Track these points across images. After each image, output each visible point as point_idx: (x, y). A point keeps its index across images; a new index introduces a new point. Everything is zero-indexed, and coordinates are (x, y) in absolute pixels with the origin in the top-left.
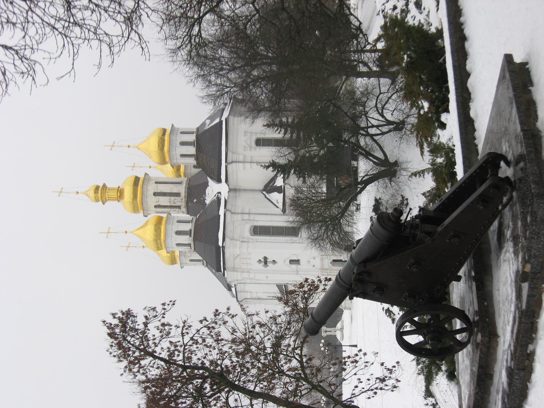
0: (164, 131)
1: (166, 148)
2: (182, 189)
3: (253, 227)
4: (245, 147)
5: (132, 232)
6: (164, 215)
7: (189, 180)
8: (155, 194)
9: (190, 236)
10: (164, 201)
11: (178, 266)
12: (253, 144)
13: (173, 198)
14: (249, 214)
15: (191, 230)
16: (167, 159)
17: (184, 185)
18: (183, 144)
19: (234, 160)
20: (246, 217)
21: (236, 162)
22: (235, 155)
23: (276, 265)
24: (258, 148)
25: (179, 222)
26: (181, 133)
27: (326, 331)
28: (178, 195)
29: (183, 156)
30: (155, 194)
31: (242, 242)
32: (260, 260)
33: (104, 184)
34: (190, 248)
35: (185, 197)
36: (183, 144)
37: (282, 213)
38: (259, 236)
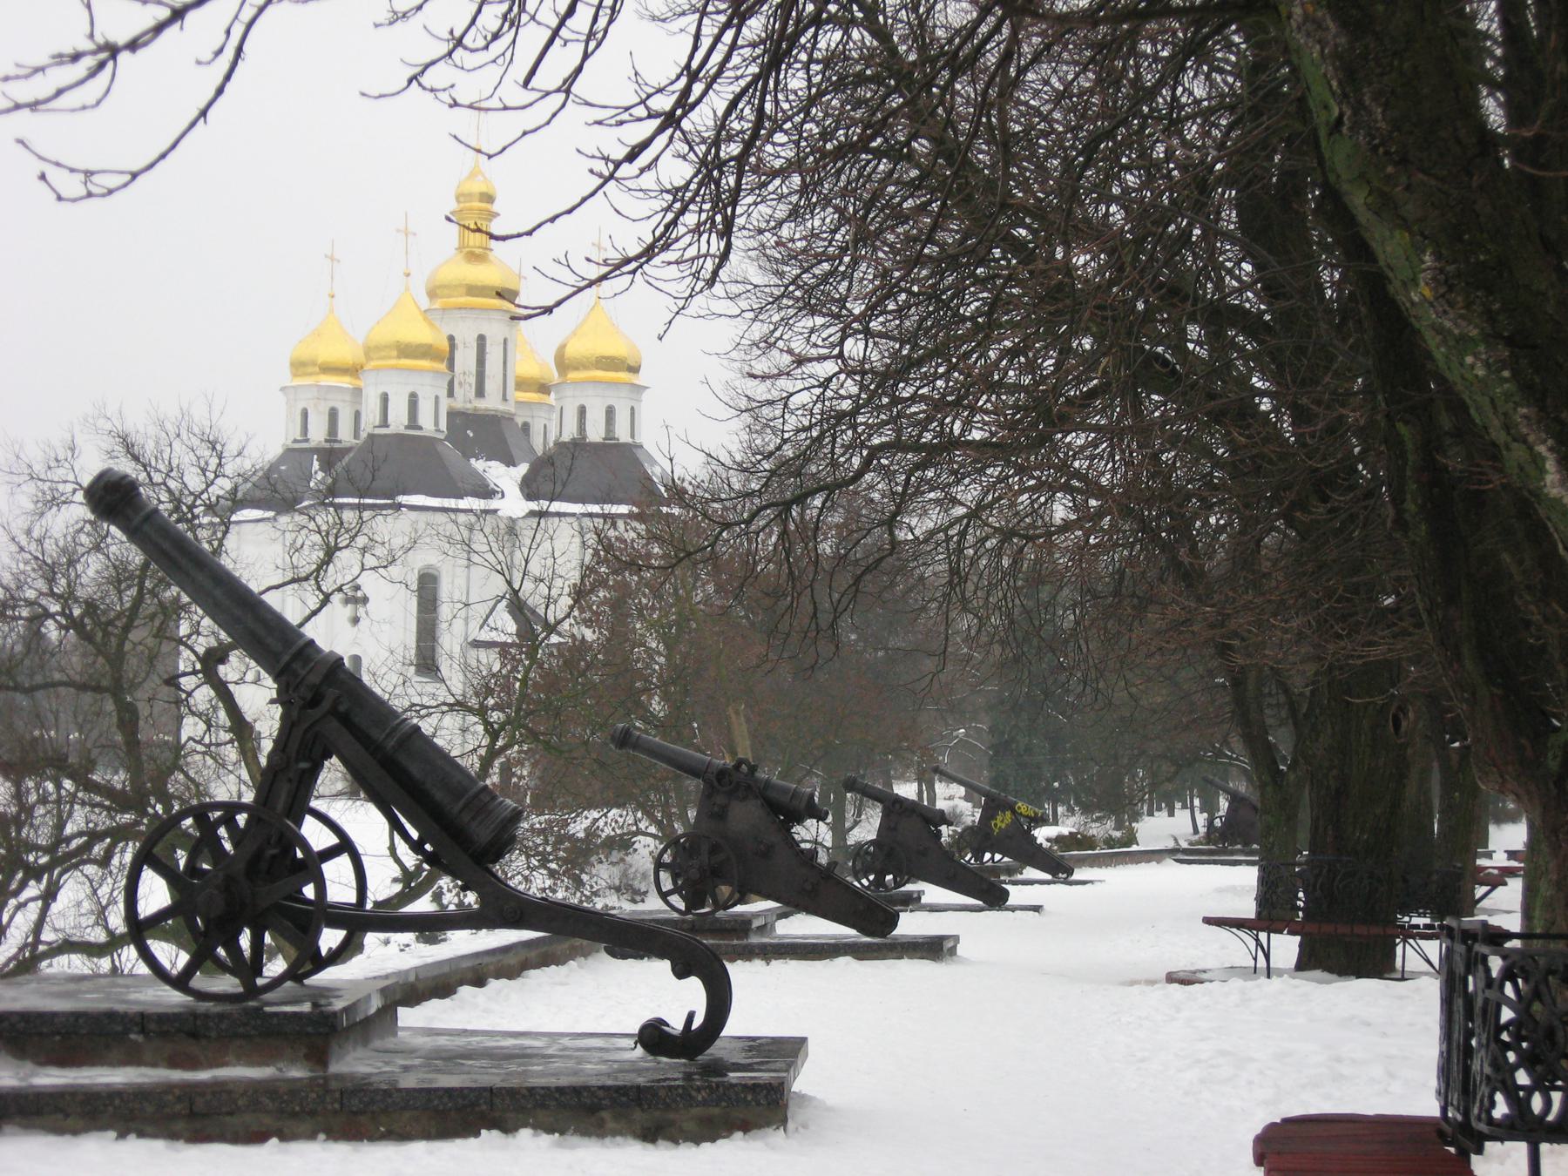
0: (634, 370)
1: (600, 374)
2: (491, 403)
3: (435, 573)
5: (407, 289)
7: (510, 418)
8: (481, 339)
9: (407, 427)
10: (466, 360)
11: (287, 379)
13: (473, 380)
15: (420, 428)
16: (572, 375)
17: (501, 407)
18: (610, 412)
23: (348, 625)
26: (632, 409)
30: (481, 339)
34: (377, 423)
35: (475, 409)
36: (610, 412)
37: (470, 640)
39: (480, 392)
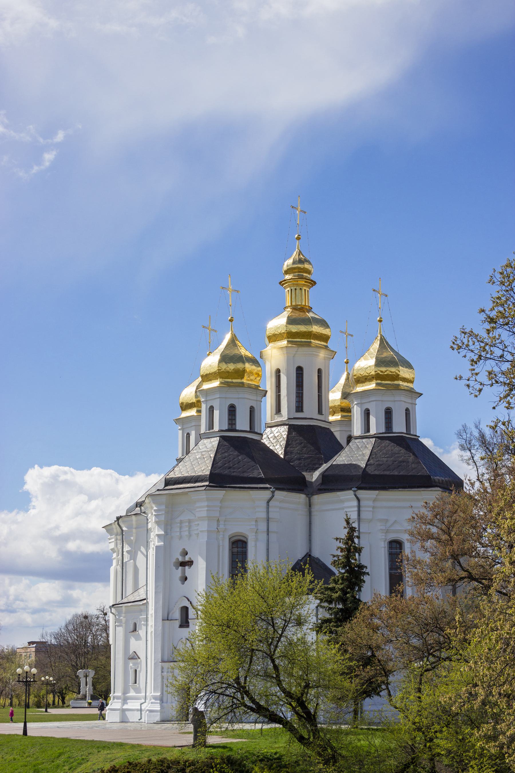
4: (387, 521)
12: (392, 536)
19: (362, 503)
20: (263, 526)
21: (359, 507)
22: (371, 503)
23: (179, 582)
25: (252, 410)
26: (407, 410)
27: (86, 676)
31: (218, 521)
33: (315, 283)
36: (388, 413)
38: (230, 550)
39: (300, 408)
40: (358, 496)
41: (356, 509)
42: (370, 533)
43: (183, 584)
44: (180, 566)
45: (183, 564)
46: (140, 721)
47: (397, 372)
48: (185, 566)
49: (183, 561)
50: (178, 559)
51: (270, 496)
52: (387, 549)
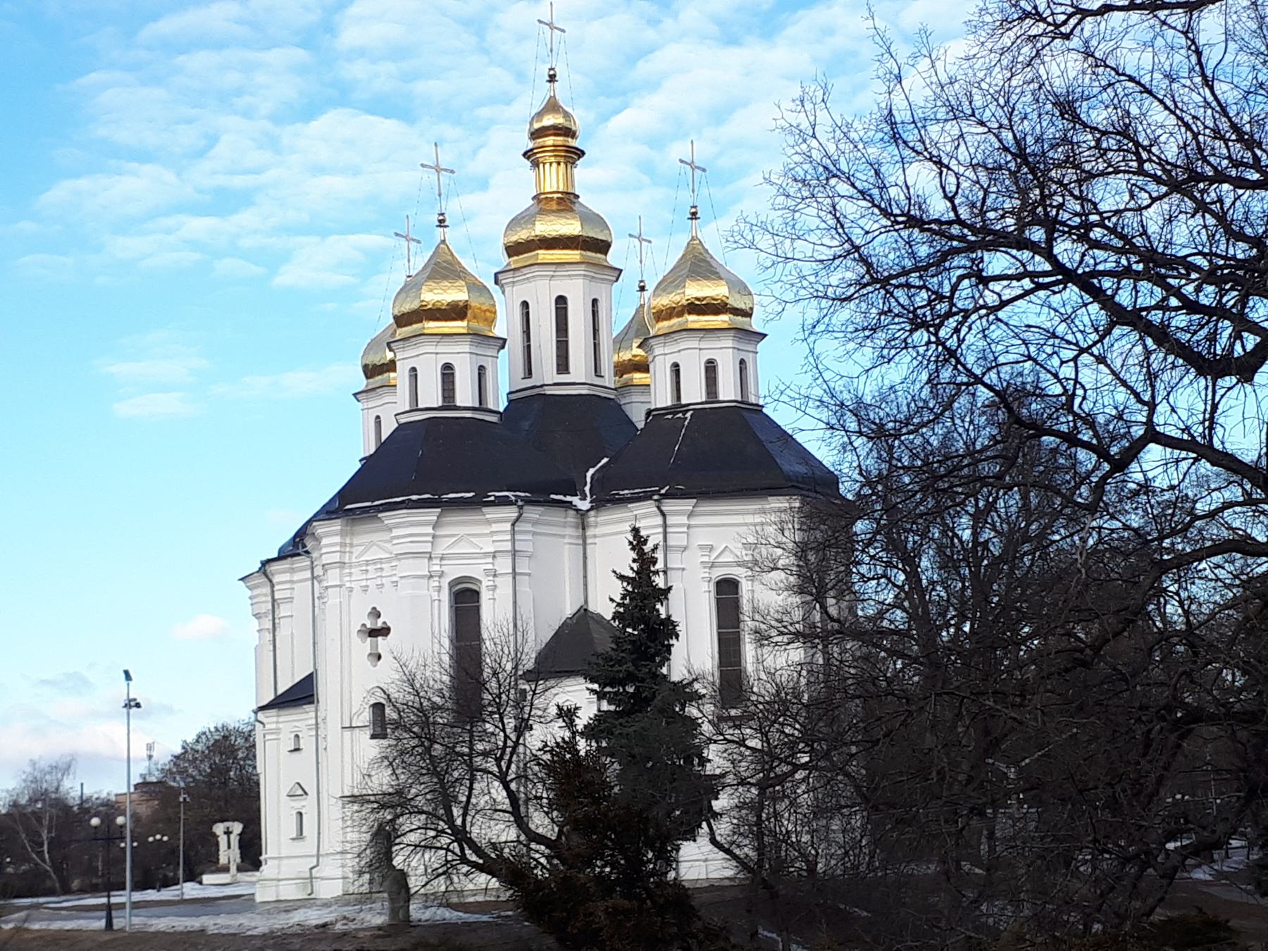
1: (694, 320)
4: (711, 548)
6: (499, 330)
14: (514, 574)
18: (711, 367)
19: (670, 520)
20: (504, 565)
21: (665, 526)
22: (684, 520)
24: (712, 588)
26: (742, 362)
28: (563, 366)
29: (676, 369)
31: (430, 558)
32: (379, 616)
34: (408, 408)
36: (711, 367)
40: (663, 508)
41: (661, 530)
42: (683, 569)
43: (375, 666)
44: (370, 636)
45: (374, 633)
46: (312, 896)
47: (724, 299)
48: (376, 636)
49: (374, 627)
50: (364, 625)
51: (516, 515)
52: (713, 594)
